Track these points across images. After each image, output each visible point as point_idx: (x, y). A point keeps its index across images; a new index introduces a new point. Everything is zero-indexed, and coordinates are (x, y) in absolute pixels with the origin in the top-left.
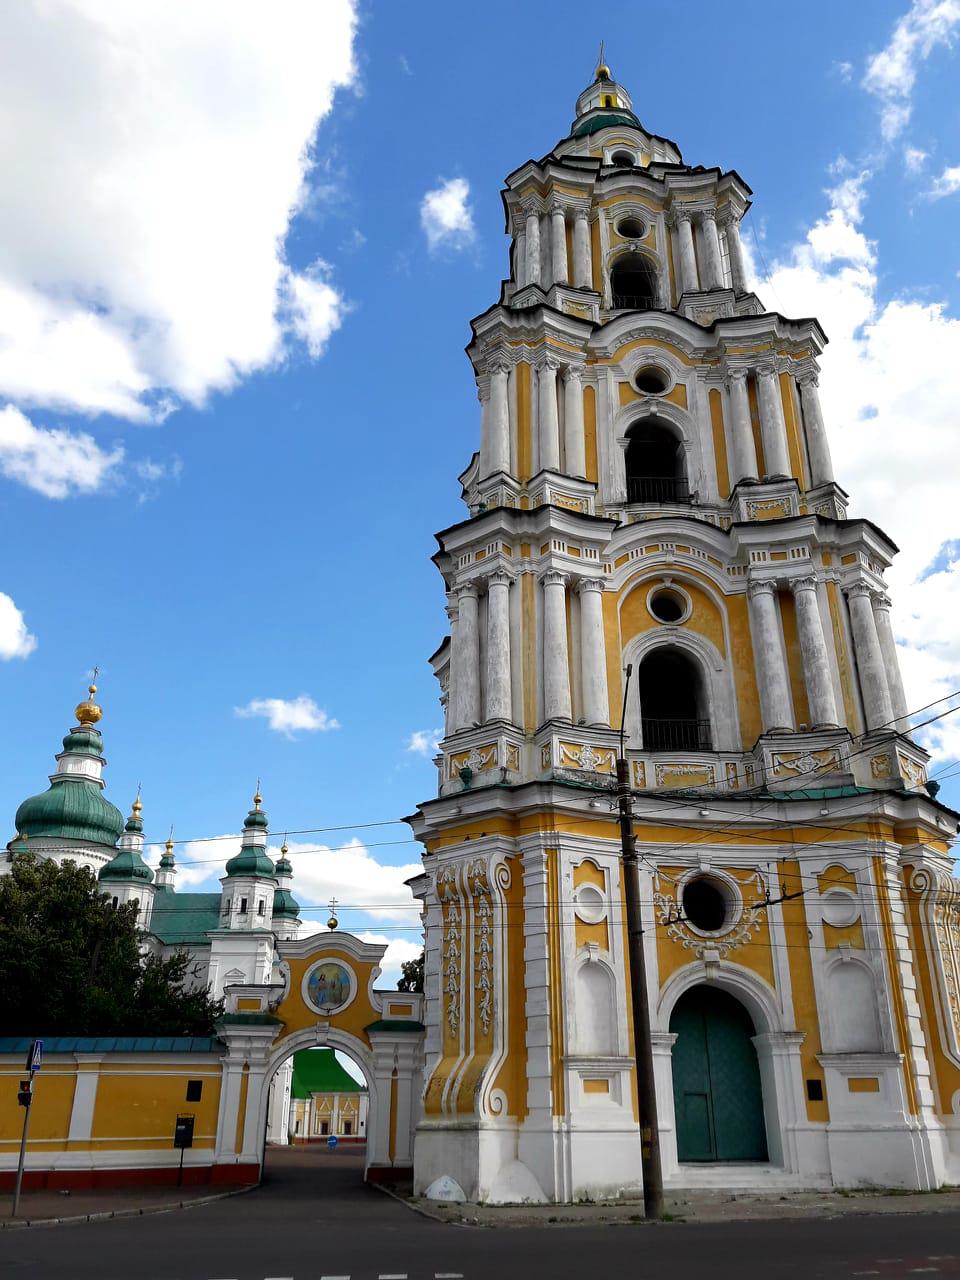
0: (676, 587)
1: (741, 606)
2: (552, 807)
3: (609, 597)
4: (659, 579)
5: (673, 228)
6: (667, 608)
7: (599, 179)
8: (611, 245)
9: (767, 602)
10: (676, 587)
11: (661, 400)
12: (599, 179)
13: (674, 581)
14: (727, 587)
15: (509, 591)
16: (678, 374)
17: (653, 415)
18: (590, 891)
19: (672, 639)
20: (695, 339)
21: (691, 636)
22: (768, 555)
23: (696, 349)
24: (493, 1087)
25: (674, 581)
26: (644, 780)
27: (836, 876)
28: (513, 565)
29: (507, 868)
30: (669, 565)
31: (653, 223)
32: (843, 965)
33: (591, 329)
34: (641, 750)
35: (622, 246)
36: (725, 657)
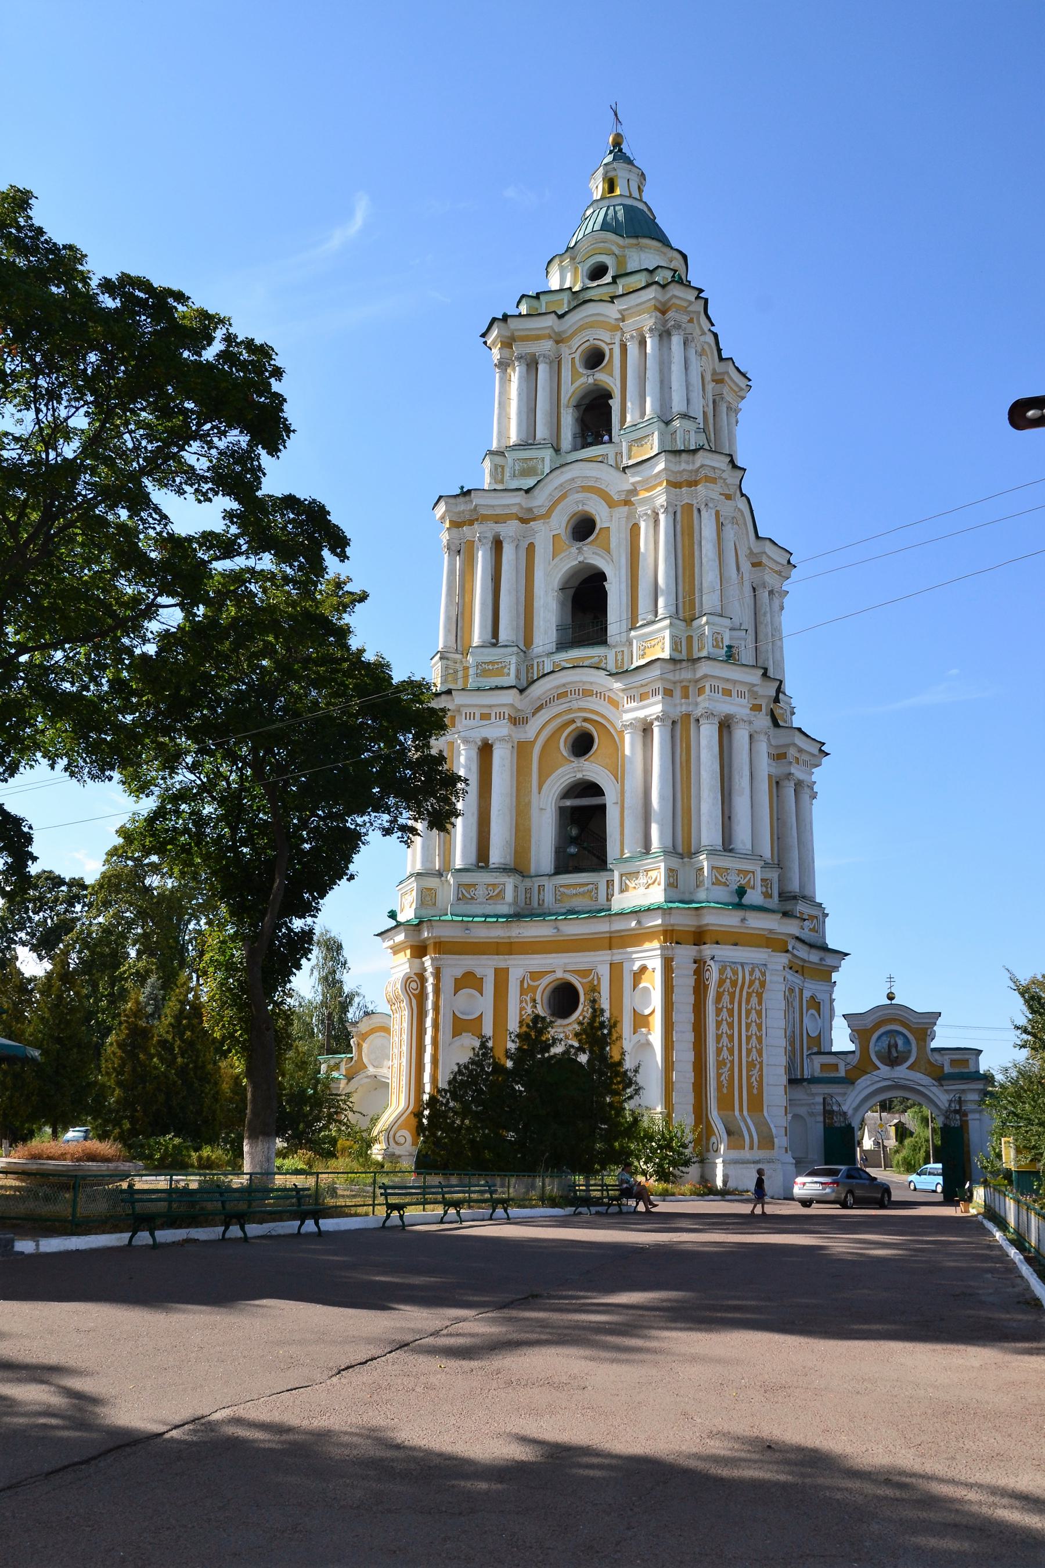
0: (585, 725)
4: (573, 721)
6: (582, 745)
8: (575, 382)
10: (585, 725)
12: (561, 317)
13: (585, 720)
19: (579, 776)
24: (400, 1128)
35: (583, 380)
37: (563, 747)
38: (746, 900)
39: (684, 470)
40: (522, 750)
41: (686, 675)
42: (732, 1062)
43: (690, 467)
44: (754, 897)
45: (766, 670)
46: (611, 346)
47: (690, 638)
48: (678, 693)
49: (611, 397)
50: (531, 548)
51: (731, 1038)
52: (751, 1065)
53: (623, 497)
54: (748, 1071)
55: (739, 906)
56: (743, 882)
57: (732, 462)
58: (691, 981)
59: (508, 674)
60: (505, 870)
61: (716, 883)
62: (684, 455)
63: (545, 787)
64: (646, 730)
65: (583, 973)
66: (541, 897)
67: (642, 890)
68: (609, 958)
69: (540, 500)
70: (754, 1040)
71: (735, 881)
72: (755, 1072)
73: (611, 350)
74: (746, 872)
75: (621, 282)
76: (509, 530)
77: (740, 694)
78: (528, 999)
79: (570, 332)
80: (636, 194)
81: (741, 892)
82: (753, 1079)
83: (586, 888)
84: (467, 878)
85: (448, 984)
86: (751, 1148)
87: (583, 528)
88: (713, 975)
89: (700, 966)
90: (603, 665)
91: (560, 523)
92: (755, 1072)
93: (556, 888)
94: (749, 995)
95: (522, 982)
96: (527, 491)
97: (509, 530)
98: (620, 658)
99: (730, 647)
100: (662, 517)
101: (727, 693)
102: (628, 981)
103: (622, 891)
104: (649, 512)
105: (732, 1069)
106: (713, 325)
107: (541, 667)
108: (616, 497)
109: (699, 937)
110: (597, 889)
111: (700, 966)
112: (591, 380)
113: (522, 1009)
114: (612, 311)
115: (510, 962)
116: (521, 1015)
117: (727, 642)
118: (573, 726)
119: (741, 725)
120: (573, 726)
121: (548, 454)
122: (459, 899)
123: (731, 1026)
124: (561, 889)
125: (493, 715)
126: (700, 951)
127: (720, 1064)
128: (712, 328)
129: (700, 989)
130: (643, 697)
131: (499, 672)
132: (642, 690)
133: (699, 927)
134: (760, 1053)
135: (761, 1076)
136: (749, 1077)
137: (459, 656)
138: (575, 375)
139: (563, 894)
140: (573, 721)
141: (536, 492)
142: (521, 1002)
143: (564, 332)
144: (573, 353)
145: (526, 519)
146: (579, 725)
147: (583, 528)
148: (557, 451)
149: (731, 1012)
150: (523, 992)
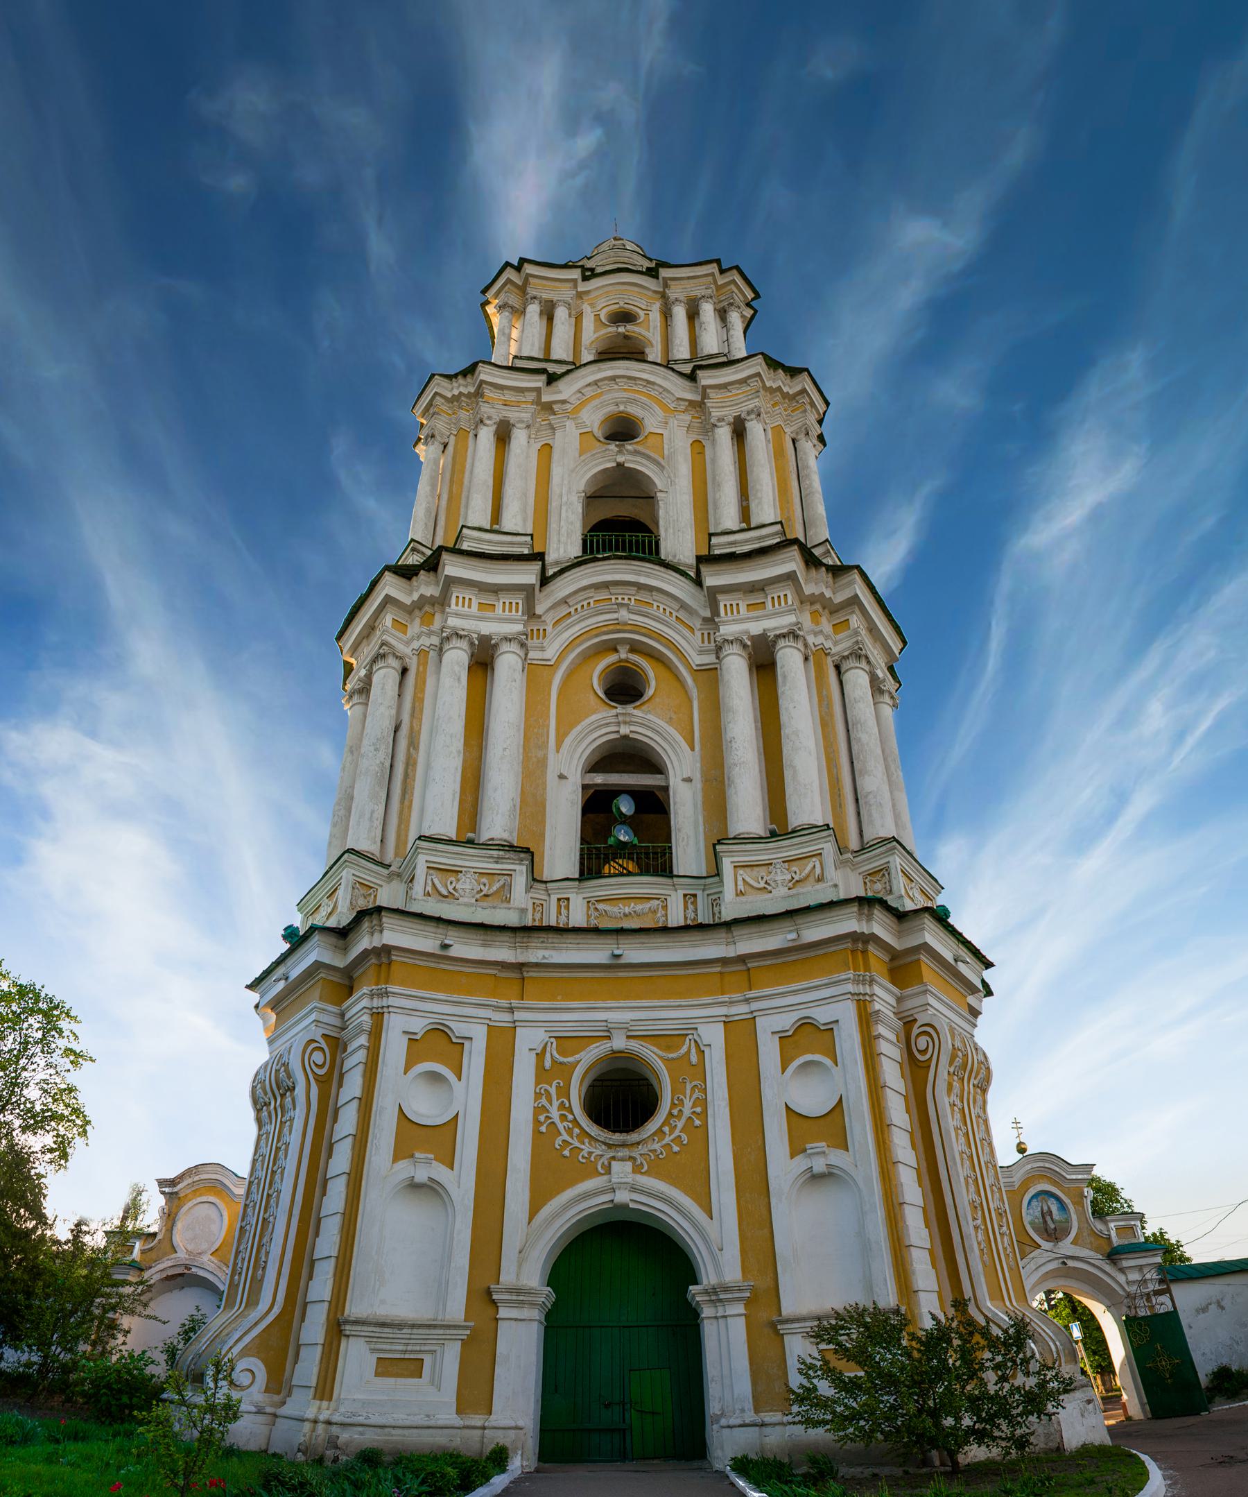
1: (711, 676)
2: (387, 950)
3: (535, 673)
6: (625, 689)
9: (736, 668)
14: (697, 659)
16: (651, 422)
18: (435, 1077)
19: (624, 730)
21: (649, 723)
22: (743, 609)
23: (678, 399)
25: (632, 650)
28: (408, 643)
29: (324, 1045)
32: (815, 1178)
33: (544, 377)
36: (693, 749)
65: (667, 1040)
67: (783, 891)
68: (723, 1010)
69: (567, 389)
76: (521, 414)
78: (553, 1090)
85: (394, 1048)
95: (540, 1056)
97: (521, 414)
103: (740, 894)
108: (672, 406)
113: (539, 1110)
115: (518, 1015)
116: (537, 1123)
118: (612, 658)
120: (612, 658)
141: (561, 384)
142: (538, 1095)
146: (623, 656)
150: (542, 1074)
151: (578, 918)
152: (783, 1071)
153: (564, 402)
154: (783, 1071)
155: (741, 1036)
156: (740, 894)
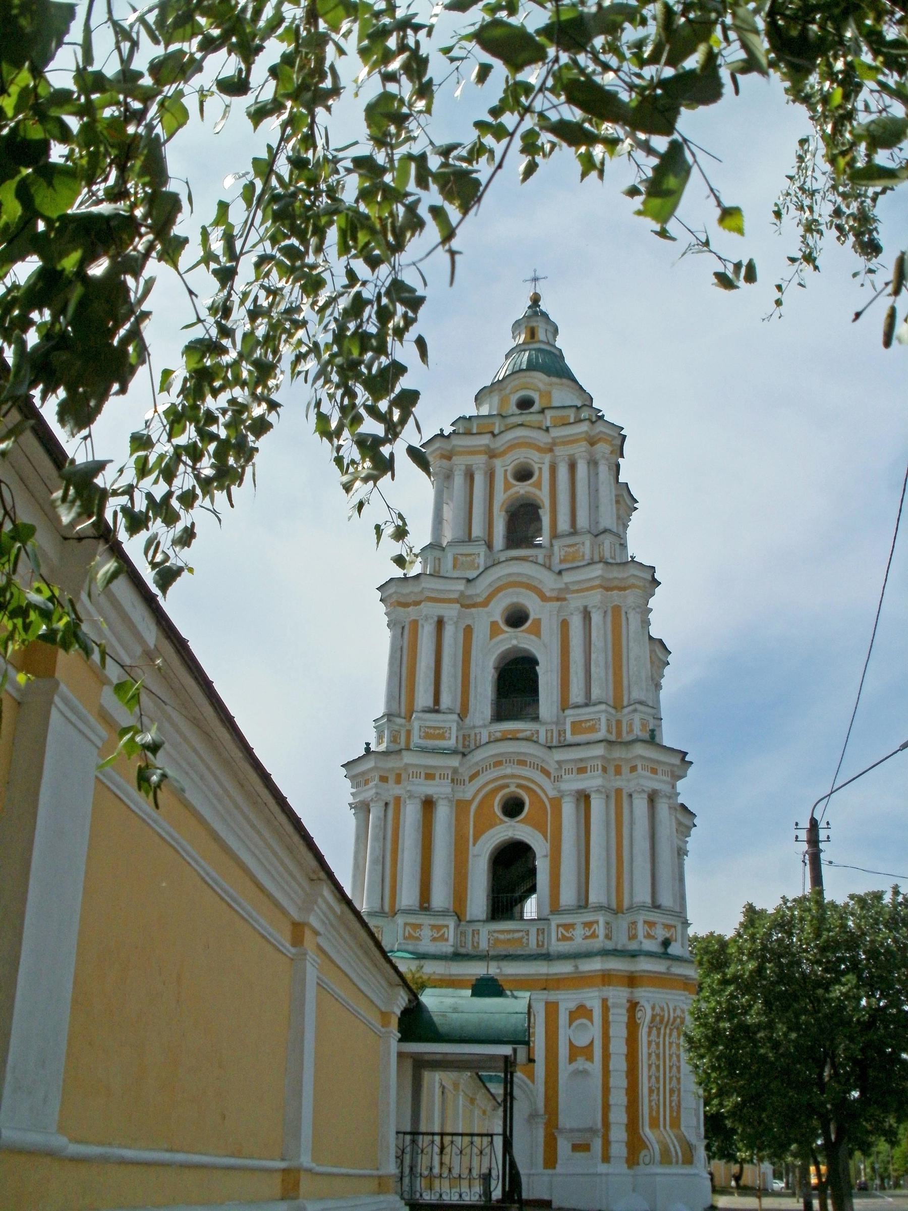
5: (553, 470)
6: (513, 808)
7: (494, 435)
11: (520, 634)
13: (519, 786)
14: (552, 793)
15: (385, 810)
17: (515, 647)
20: (549, 582)
23: (553, 590)
25: (519, 786)
26: (478, 943)
27: (581, 1012)
30: (513, 776)
31: (540, 465)
34: (484, 921)
37: (498, 811)
38: (672, 950)
39: (615, 578)
40: (461, 807)
41: (618, 753)
42: (658, 1089)
43: (620, 576)
44: (675, 949)
45: (685, 754)
46: (540, 465)
47: (619, 722)
48: (611, 770)
49: (540, 508)
50: (468, 631)
51: (658, 1067)
52: (672, 1091)
53: (554, 594)
54: (671, 1096)
55: (665, 955)
56: (668, 935)
57: (653, 576)
58: (625, 1019)
59: (450, 738)
60: (444, 913)
61: (649, 936)
62: (615, 567)
63: (479, 842)
64: (584, 798)
66: (476, 939)
68: (544, 997)
69: (481, 588)
70: (675, 1069)
71: (661, 933)
72: (675, 1098)
73: (540, 469)
74: (668, 927)
75: (549, 414)
76: (450, 612)
77: (664, 773)
79: (502, 449)
80: (551, 341)
81: (666, 943)
82: (673, 1104)
83: (517, 935)
84: (412, 919)
86: (677, 1162)
87: (517, 618)
88: (645, 1016)
89: (633, 1006)
90: (535, 738)
91: (497, 610)
92: (675, 1098)
93: (487, 935)
94: (671, 1030)
96: (469, 581)
97: (450, 612)
98: (549, 735)
99: (653, 731)
100: (596, 618)
101: (654, 771)
102: (563, 1018)
103: (558, 940)
104: (582, 608)
105: (658, 1095)
106: (622, 456)
107: (478, 737)
108: (548, 594)
109: (632, 980)
110: (528, 935)
111: (633, 1006)
112: (522, 492)
114: (543, 438)
117: (651, 727)
118: (507, 791)
119: (664, 800)
120: (507, 791)
121: (482, 550)
122: (405, 938)
123: (658, 1056)
124: (496, 935)
125: (437, 776)
126: (632, 992)
127: (651, 1091)
128: (620, 460)
129: (633, 1026)
130: (582, 770)
131: (442, 737)
132: (582, 765)
133: (632, 972)
134: (679, 1080)
135: (679, 1102)
136: (671, 1102)
137: (403, 721)
138: (507, 486)
139: (497, 940)
140: (507, 786)
143: (497, 448)
144: (504, 467)
145: (466, 603)
146: (513, 788)
147: (517, 618)
148: (489, 546)
149: (658, 1044)
151: (484, 945)
152: (570, 1025)
153: (477, 595)
154: (570, 1025)
155: (552, 1009)
156: (558, 940)
